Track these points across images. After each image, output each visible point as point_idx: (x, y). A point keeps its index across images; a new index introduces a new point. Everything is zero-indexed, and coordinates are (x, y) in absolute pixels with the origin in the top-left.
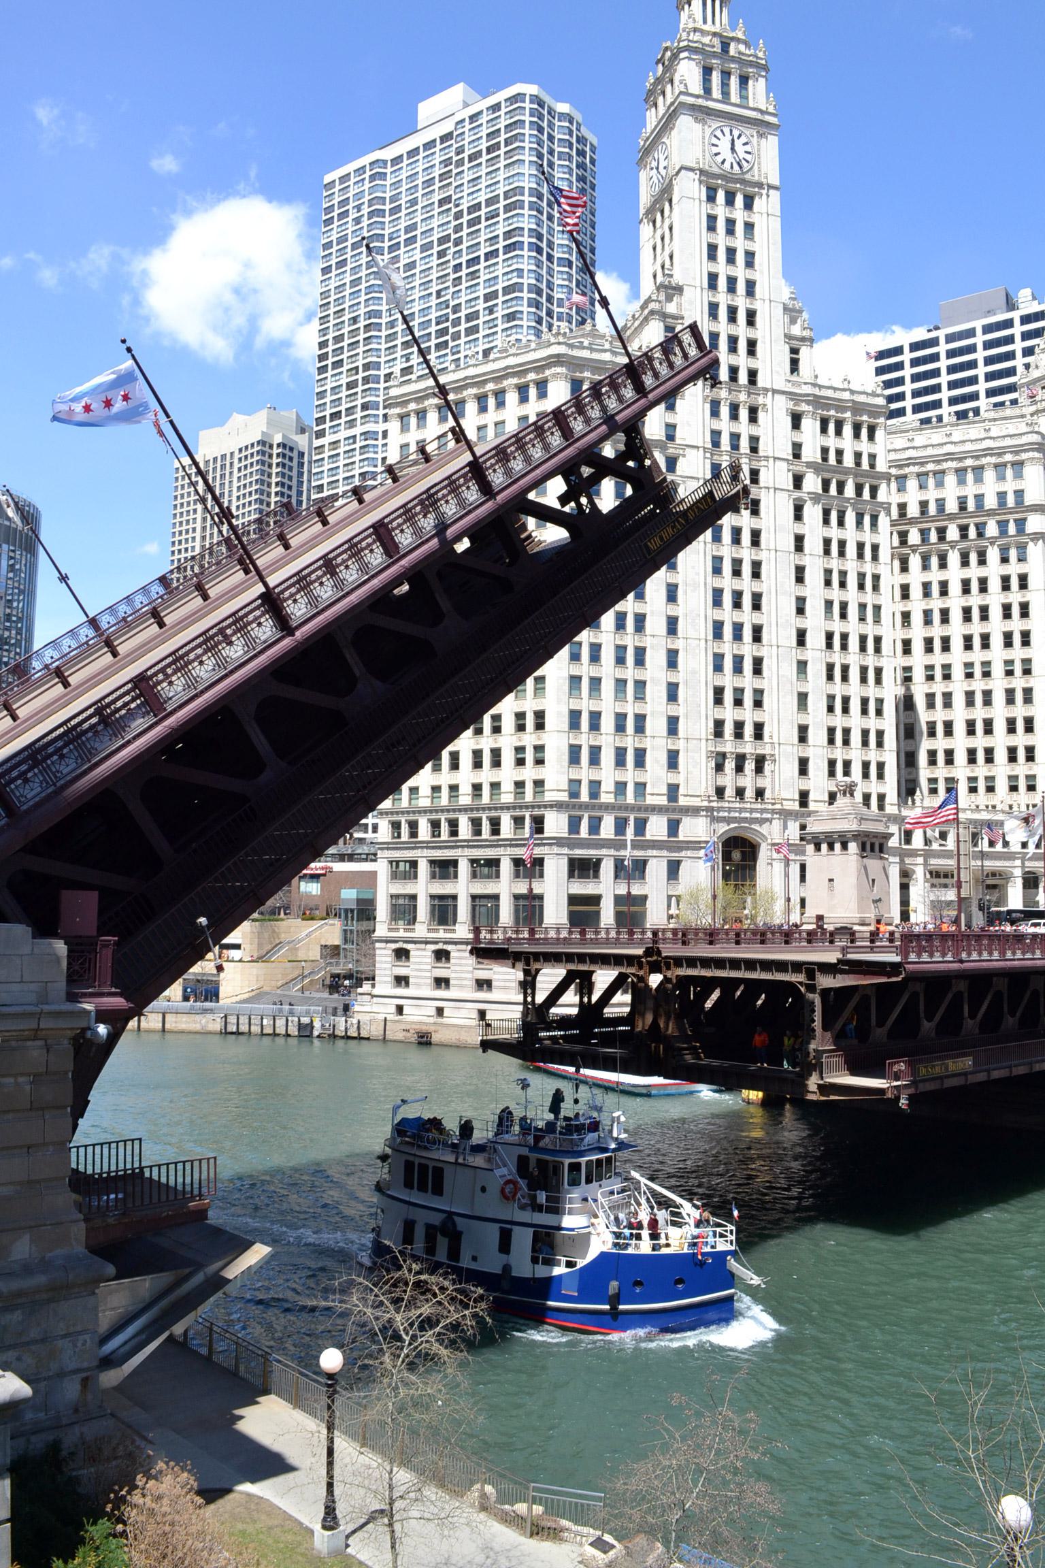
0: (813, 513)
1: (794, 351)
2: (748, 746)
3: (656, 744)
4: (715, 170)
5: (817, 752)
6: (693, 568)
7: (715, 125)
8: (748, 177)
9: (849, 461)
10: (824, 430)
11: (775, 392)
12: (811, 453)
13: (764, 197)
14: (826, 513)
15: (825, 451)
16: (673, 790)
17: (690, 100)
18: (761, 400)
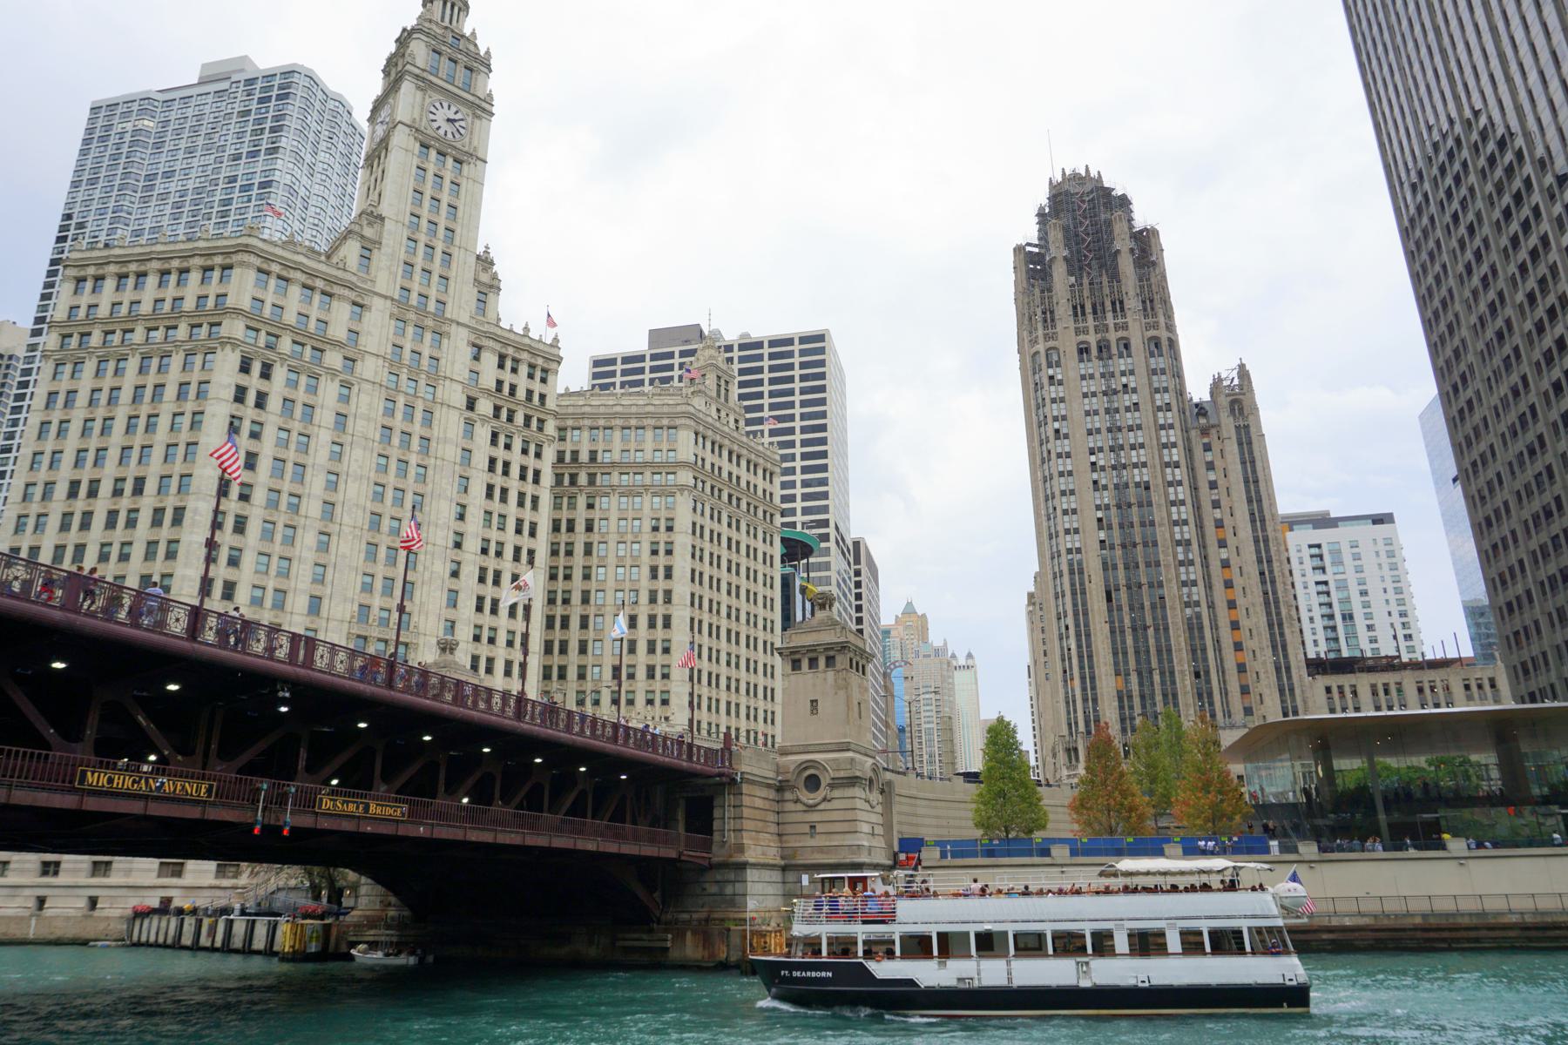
4: (429, 132)
6: (357, 461)
7: (436, 96)
8: (458, 145)
9: (521, 394)
10: (501, 366)
11: (458, 323)
13: (472, 166)
14: (495, 435)
15: (500, 383)
17: (417, 71)
18: (445, 328)
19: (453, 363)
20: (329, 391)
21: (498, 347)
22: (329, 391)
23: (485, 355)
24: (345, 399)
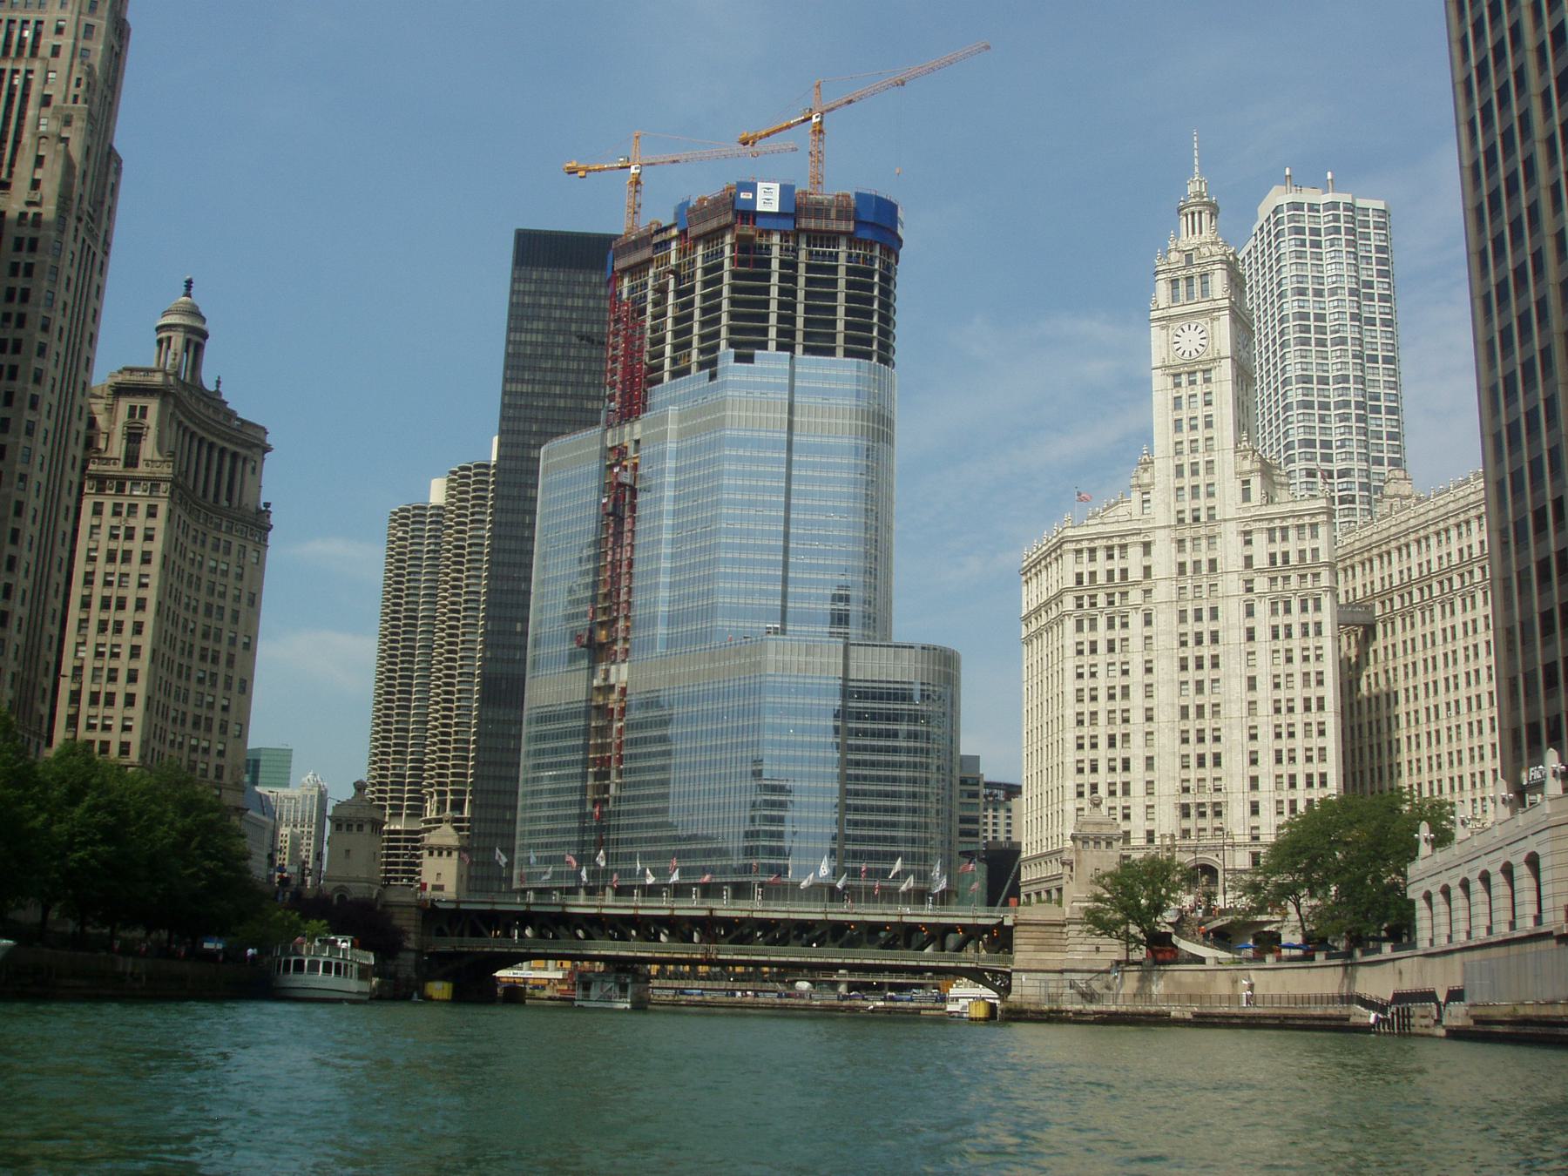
0: (1262, 608)
1: (1246, 482)
2: (1207, 798)
4: (1179, 362)
14: (1274, 604)
19: (1226, 558)
20: (1136, 620)
21: (1265, 525)
22: (1136, 620)
23: (1255, 537)
24: (1148, 622)
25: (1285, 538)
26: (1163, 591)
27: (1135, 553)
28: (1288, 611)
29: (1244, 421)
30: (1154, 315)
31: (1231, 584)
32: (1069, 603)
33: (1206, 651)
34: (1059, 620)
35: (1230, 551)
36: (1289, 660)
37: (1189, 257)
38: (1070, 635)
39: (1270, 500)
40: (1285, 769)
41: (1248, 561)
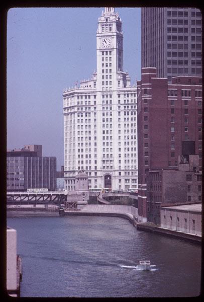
0: (122, 113)
1: (119, 81)
3: (93, 160)
4: (103, 48)
5: (123, 159)
8: (110, 48)
12: (122, 102)
14: (125, 112)
16: (96, 167)
20: (92, 114)
21: (123, 93)
22: (92, 114)
23: (121, 95)
25: (128, 96)
26: (99, 108)
27: (92, 97)
28: (128, 114)
29: (120, 66)
30: (98, 35)
31: (115, 107)
32: (76, 109)
33: (109, 123)
34: (74, 113)
35: (115, 99)
36: (128, 138)
37: (107, 20)
38: (76, 118)
39: (125, 86)
40: (127, 146)
41: (119, 101)
